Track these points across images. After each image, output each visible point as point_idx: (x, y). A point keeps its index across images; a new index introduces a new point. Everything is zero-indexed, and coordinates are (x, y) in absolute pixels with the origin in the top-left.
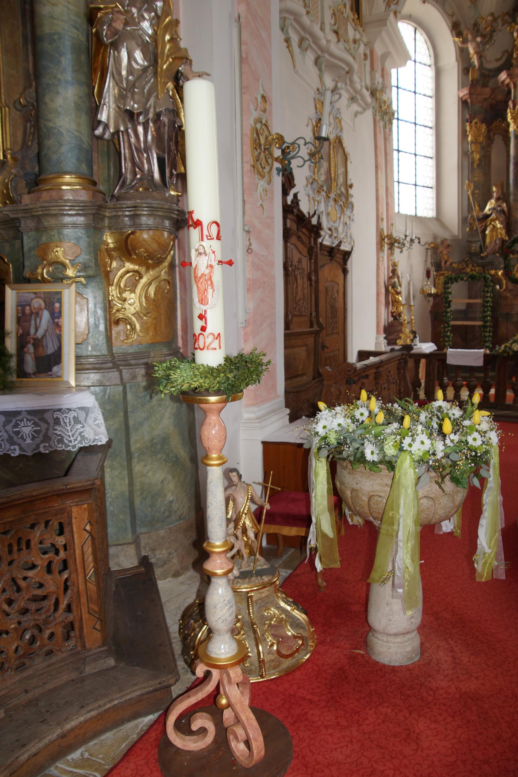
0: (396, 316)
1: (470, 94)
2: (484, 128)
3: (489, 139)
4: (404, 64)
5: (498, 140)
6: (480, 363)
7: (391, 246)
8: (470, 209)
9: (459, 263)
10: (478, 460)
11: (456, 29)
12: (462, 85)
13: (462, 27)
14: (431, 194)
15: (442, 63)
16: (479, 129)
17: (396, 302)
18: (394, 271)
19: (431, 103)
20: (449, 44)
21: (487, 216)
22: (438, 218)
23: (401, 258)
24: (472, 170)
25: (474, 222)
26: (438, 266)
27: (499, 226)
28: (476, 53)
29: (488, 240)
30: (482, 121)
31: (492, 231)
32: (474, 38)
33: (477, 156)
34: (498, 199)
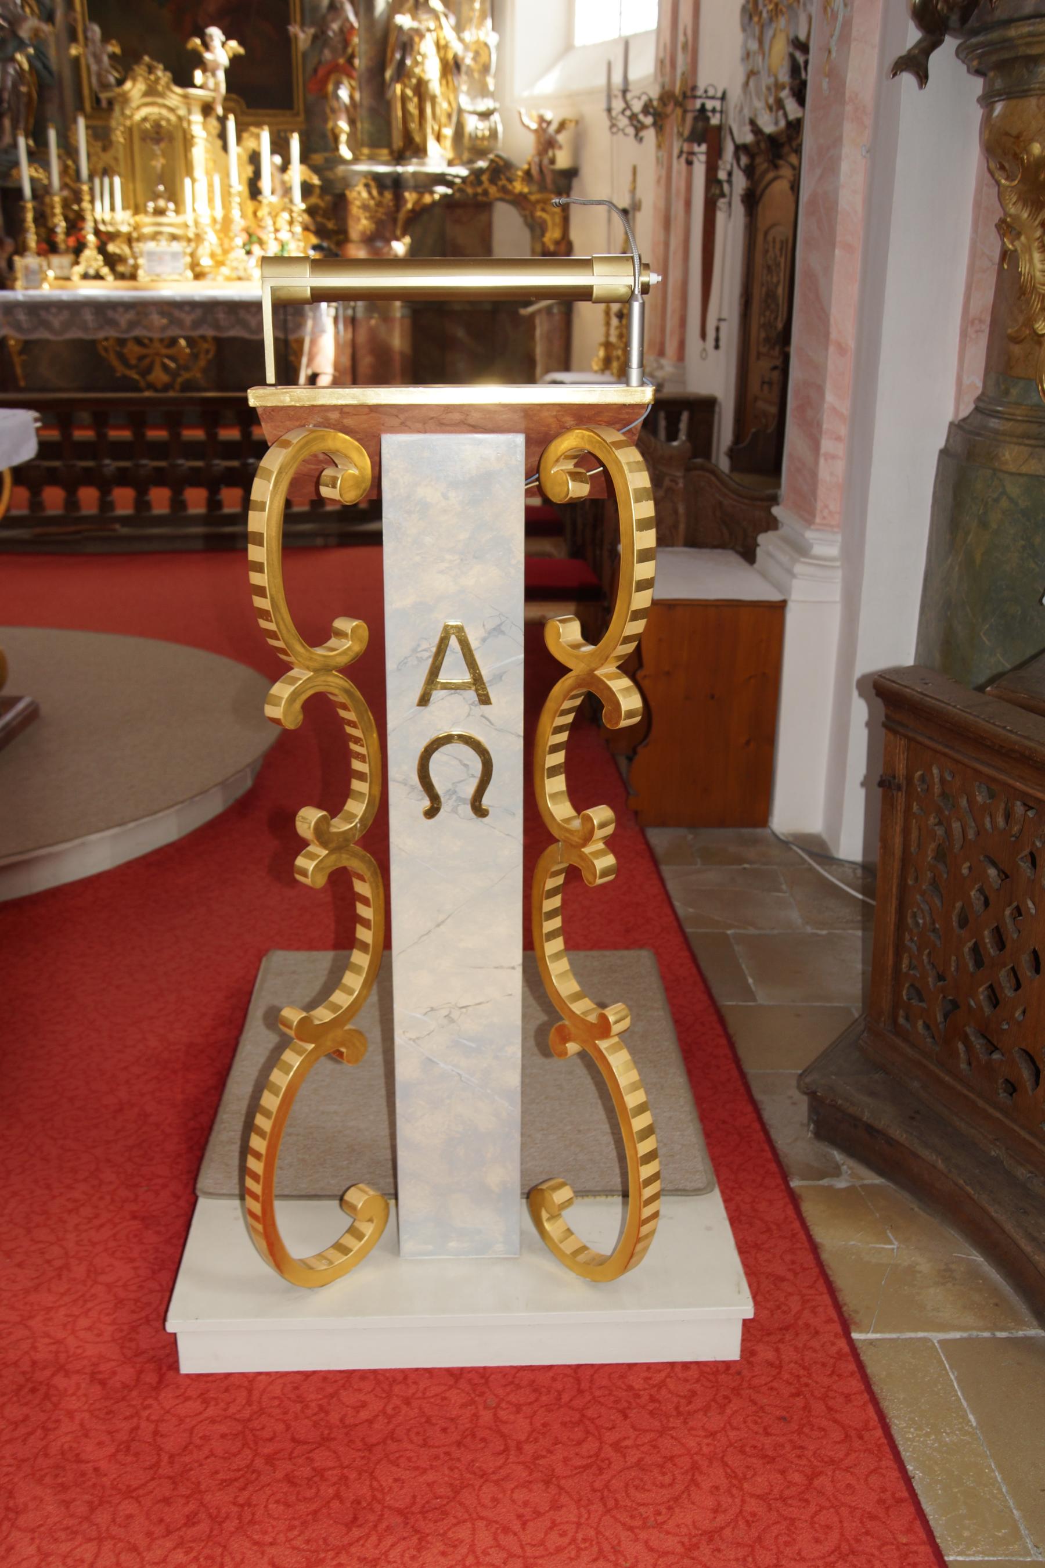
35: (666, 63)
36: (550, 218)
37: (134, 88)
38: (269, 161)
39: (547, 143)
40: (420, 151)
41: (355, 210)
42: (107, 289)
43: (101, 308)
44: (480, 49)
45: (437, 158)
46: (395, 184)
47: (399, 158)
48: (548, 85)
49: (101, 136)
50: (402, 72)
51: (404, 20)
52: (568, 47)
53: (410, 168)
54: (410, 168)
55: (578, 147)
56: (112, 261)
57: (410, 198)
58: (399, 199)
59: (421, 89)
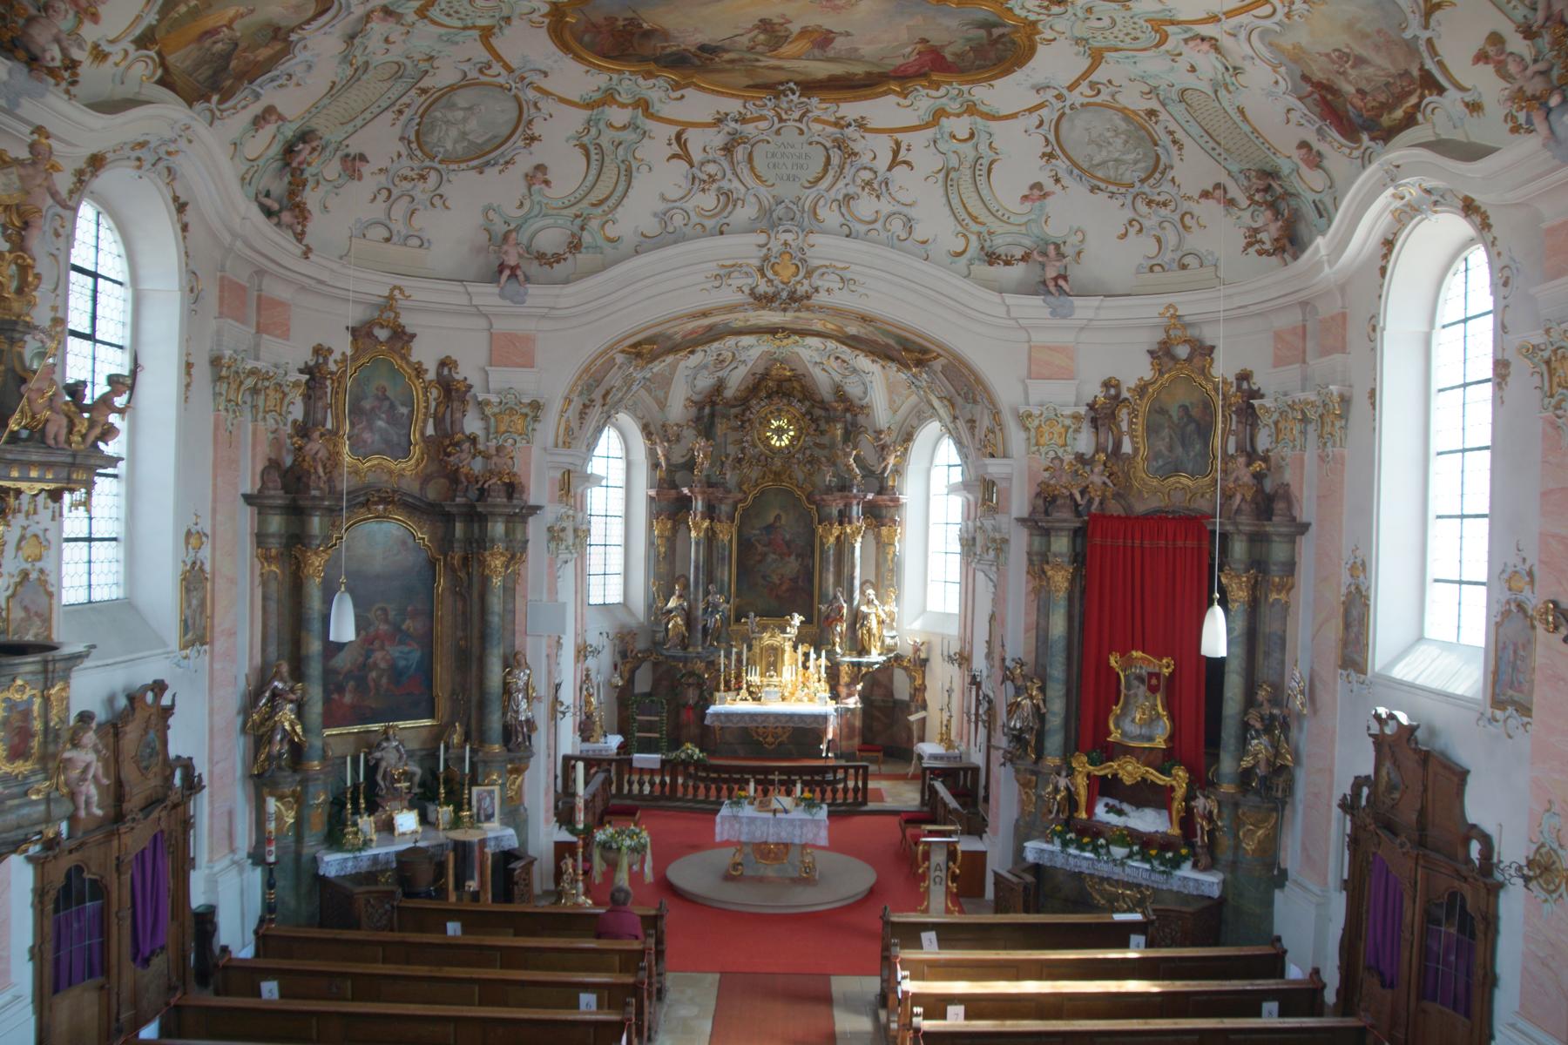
0: (589, 716)
3: (675, 530)
5: (683, 527)
6: (658, 766)
10: (644, 846)
11: (647, 431)
13: (652, 429)
15: (633, 457)
17: (588, 703)
18: (587, 676)
20: (639, 444)
21: (670, 611)
22: (625, 605)
23: (591, 662)
25: (657, 614)
26: (624, 654)
33: (662, 550)
34: (680, 596)
35: (963, 639)
36: (918, 676)
37: (766, 635)
38: (813, 656)
39: (917, 650)
40: (868, 653)
41: (843, 674)
42: (749, 706)
43: (753, 716)
44: (890, 615)
46: (859, 664)
47: (860, 654)
48: (917, 625)
51: (864, 608)
52: (924, 610)
53: (864, 660)
54: (864, 660)
55: (929, 650)
56: (751, 693)
57: (864, 670)
59: (869, 631)
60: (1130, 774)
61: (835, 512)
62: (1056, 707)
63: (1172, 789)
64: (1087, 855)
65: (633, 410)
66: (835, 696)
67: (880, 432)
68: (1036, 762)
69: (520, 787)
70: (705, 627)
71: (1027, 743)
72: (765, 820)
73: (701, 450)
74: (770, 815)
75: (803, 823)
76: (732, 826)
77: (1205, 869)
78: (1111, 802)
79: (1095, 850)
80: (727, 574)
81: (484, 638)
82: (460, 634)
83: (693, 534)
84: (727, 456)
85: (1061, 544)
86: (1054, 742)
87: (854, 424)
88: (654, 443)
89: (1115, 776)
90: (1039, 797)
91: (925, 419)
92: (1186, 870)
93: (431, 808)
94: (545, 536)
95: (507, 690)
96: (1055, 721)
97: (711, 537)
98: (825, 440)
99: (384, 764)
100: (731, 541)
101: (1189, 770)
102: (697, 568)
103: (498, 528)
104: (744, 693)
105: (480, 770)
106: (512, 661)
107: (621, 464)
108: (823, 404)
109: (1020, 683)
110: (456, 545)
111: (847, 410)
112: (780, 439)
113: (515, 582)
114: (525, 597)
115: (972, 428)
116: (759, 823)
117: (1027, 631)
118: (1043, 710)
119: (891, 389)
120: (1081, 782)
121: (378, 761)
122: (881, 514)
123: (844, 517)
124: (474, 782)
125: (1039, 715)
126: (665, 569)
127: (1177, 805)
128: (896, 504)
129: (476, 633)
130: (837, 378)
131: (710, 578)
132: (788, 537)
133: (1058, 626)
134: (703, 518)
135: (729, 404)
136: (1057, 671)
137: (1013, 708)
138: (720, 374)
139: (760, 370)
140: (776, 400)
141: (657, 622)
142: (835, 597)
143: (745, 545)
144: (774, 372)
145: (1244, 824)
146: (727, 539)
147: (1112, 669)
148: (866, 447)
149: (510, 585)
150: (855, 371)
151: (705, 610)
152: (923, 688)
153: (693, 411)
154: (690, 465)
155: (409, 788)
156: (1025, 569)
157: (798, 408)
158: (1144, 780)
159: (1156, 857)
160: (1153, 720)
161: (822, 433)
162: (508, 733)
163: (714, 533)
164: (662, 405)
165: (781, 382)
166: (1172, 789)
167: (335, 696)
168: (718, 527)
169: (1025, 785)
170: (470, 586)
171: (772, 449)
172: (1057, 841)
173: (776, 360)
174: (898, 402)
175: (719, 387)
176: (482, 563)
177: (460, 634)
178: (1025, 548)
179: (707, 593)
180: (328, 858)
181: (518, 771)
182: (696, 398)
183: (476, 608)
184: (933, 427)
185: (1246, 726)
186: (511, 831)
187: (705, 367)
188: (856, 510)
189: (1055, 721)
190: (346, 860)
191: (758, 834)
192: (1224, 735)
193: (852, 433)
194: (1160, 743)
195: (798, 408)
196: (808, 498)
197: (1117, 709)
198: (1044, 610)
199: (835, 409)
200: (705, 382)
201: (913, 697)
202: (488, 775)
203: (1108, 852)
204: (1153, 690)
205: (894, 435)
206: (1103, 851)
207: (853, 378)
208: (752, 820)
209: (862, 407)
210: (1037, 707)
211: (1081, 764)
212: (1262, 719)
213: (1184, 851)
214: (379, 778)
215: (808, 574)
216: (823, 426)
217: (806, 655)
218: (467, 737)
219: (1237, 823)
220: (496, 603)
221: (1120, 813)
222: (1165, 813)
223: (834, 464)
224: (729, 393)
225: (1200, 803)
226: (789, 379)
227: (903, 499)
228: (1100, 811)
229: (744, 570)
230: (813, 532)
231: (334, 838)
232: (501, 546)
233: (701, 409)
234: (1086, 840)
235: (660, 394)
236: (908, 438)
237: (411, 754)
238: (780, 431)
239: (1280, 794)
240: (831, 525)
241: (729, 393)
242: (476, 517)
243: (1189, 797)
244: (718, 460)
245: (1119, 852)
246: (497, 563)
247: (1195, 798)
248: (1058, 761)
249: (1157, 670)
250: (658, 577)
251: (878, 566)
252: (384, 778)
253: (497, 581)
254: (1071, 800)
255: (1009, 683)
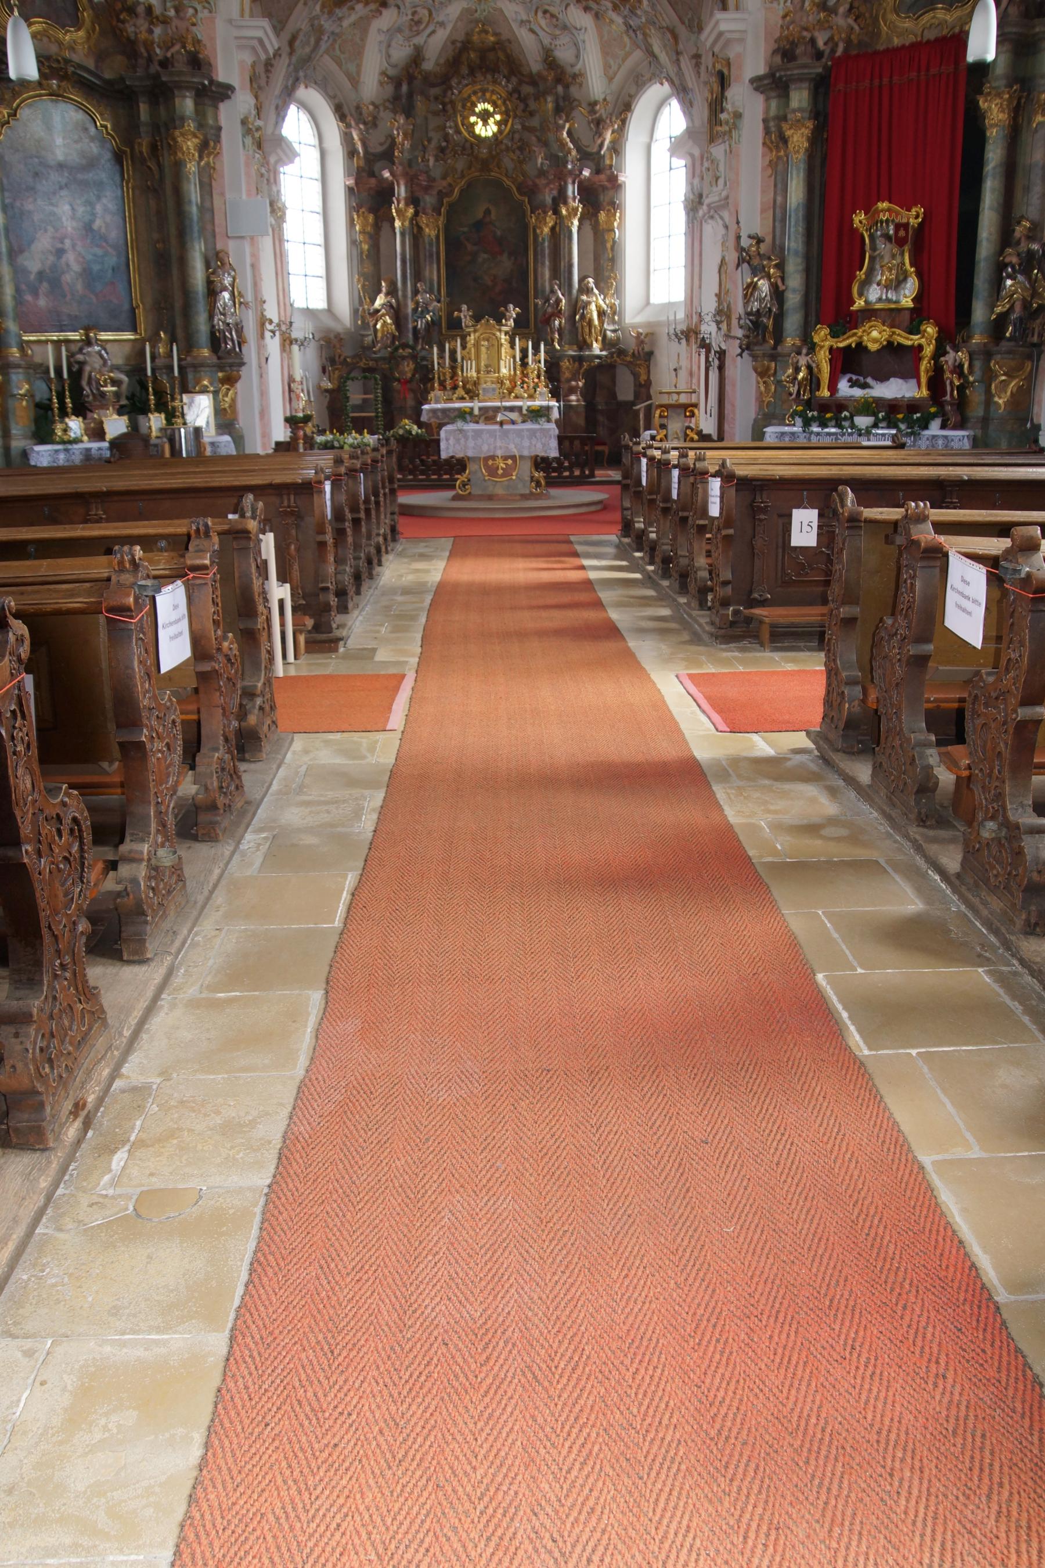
1: (357, 183)
2: (371, 218)
3: (377, 226)
4: (292, 162)
5: (386, 226)
7: (291, 343)
8: (361, 303)
9: (353, 357)
12: (348, 173)
13: (346, 110)
14: (322, 284)
15: (327, 145)
16: (366, 218)
19: (317, 186)
21: (377, 311)
22: (330, 310)
24: (361, 261)
25: (364, 316)
26: (332, 361)
27: (389, 321)
28: (361, 140)
29: (379, 335)
30: (371, 210)
31: (383, 326)
32: (357, 124)
33: (366, 247)
34: (387, 294)
35: (689, 316)
36: (642, 371)
40: (590, 347)
44: (612, 306)
45: (596, 348)
47: (581, 349)
49: (464, 347)
50: (583, 317)
51: (584, 298)
55: (653, 343)
56: (468, 392)
58: (581, 366)
59: (590, 322)
60: (875, 341)
61: (549, 200)
62: (795, 282)
63: (920, 348)
64: (833, 430)
65: (324, 85)
66: (555, 394)
67: (595, 103)
68: (775, 348)
69: (233, 400)
70: (415, 328)
71: (766, 327)
72: (492, 433)
73: (396, 127)
74: (497, 427)
75: (533, 433)
76: (458, 441)
77: (955, 428)
78: (854, 377)
79: (839, 425)
80: (433, 272)
81: (182, 233)
82: (156, 236)
83: (397, 224)
84: (429, 141)
85: (800, 98)
86: (792, 323)
87: (567, 98)
88: (348, 126)
89: (859, 344)
90: (779, 383)
91: (644, 84)
92: (935, 428)
93: (141, 419)
94: (239, 129)
95: (212, 292)
96: (793, 299)
97: (415, 233)
98: (535, 122)
99: (87, 368)
100: (438, 237)
101: (937, 324)
102: (404, 261)
103: (187, 105)
104: (460, 392)
105: (190, 376)
106: (216, 261)
107: (316, 154)
108: (534, 80)
109: (756, 262)
110: (142, 129)
111: (559, 80)
112: (485, 123)
113: (210, 177)
114: (223, 194)
115: (697, 65)
116: (485, 436)
117: (763, 211)
118: (782, 288)
119: (606, 50)
120: (823, 358)
121: (82, 364)
122: (601, 197)
123: (561, 198)
124: (185, 389)
125: (778, 294)
126: (371, 264)
127: (924, 365)
128: (614, 185)
129: (173, 231)
130: (547, 41)
131: (418, 276)
132: (499, 233)
133: (796, 193)
134: (407, 205)
135: (428, 80)
136: (794, 242)
137: (751, 289)
138: (419, 40)
139: (460, 37)
140: (479, 77)
141: (365, 325)
142: (553, 291)
143: (453, 244)
144: (475, 38)
145: (997, 376)
146: (433, 233)
147: (855, 232)
148: (580, 121)
149: (206, 180)
150: (565, 28)
151: (415, 310)
152: (648, 384)
153: (390, 89)
154: (387, 156)
155: (117, 395)
156: (761, 141)
157: (503, 87)
158: (890, 343)
159: (902, 421)
160: (897, 284)
161: (532, 114)
162: (216, 341)
163: (420, 229)
164: (355, 81)
165: (484, 52)
166: (920, 348)
167: (29, 298)
168: (423, 220)
169: (762, 373)
170: (162, 179)
171: (478, 138)
172: (799, 421)
173: (477, 21)
174: (614, 67)
175: (417, 58)
176: (174, 148)
177: (156, 236)
178: (761, 117)
179: (416, 292)
180: (37, 448)
181: (231, 380)
182: (391, 72)
183: (171, 203)
184: (656, 91)
185: (999, 269)
186: (227, 438)
187: (399, 30)
188: (572, 190)
189: (793, 299)
190: (57, 451)
191: (485, 448)
192: (976, 281)
193: (565, 107)
194: (907, 302)
195: (503, 87)
196: (518, 189)
197: (861, 275)
198: (781, 186)
199: (545, 79)
200: (401, 53)
201: (637, 395)
202: (198, 382)
203: (853, 426)
204: (900, 242)
205: (610, 107)
206: (846, 424)
207: (564, 39)
208: (478, 434)
209: (575, 76)
210: (774, 287)
211: (821, 335)
212: (1019, 255)
213: (933, 410)
214: (84, 383)
215: (523, 274)
216: (533, 105)
217: (524, 352)
218: (173, 339)
219: (988, 376)
220: (193, 193)
221: (865, 386)
222: (914, 382)
223: (546, 144)
224: (428, 65)
225: (951, 358)
226: (493, 49)
227: (621, 179)
228: (844, 388)
229: (454, 273)
230: (525, 227)
231: (43, 434)
232: (191, 125)
233: (398, 85)
234: (828, 415)
235: (352, 68)
236: (627, 107)
237: (115, 368)
238: (485, 116)
239: (1035, 339)
240: (545, 213)
241: (428, 65)
242: (161, 93)
243: (939, 352)
244: (420, 144)
245: (863, 421)
246: (190, 145)
247: (945, 353)
248: (798, 342)
249: (905, 221)
250: (361, 274)
251: (597, 259)
252: (89, 383)
253: (192, 167)
254: (813, 381)
255: (745, 266)
